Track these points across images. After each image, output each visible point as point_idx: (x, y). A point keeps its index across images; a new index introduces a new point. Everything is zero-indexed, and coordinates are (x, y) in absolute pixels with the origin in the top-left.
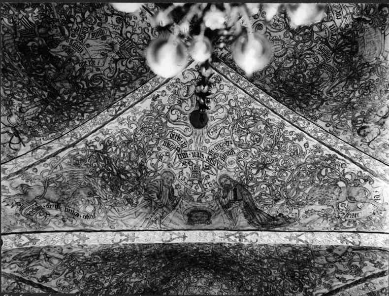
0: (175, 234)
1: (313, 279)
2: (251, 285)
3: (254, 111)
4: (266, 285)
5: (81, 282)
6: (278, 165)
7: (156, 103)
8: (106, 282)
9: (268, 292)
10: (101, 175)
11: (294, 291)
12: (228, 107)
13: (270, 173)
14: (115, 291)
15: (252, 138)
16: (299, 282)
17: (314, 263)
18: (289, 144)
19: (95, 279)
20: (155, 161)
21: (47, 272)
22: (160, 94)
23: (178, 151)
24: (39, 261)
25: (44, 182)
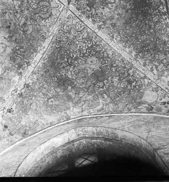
1: (147, 56)
4: (133, 35)
11: (135, 49)
17: (159, 54)
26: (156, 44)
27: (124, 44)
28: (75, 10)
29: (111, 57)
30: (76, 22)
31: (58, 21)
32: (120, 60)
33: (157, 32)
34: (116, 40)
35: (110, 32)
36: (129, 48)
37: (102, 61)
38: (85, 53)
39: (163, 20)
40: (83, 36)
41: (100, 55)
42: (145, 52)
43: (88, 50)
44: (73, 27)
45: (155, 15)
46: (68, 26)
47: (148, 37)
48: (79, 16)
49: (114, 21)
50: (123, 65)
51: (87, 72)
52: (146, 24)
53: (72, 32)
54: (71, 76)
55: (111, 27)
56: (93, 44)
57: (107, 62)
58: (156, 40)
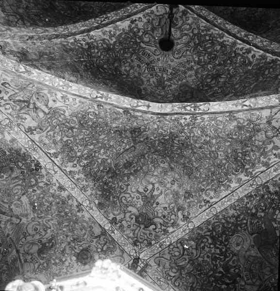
0: (141, 102)
1: (253, 158)
2: (199, 171)
3: (212, 36)
6: (229, 74)
7: (133, 26)
8: (79, 151)
9: (214, 177)
10: (84, 63)
12: (191, 35)
13: (222, 80)
14: (85, 162)
15: (209, 57)
16: (242, 163)
17: (255, 140)
18: (239, 57)
19: (71, 145)
20: (128, 69)
21: (34, 124)
22: (137, 19)
23: (148, 65)
24: (29, 110)
25: (40, 53)
26: (236, 141)
27: (222, 188)
28: (150, 251)
29: (239, 213)
30: (169, 253)
31: (160, 283)
32: (248, 201)
33: (218, 134)
34: (212, 198)
35: (197, 203)
36: (231, 182)
37: (241, 228)
38: (220, 251)
39: (203, 123)
40: (193, 248)
41: (230, 228)
42: (245, 159)
43: (217, 246)
44: (175, 260)
45: (191, 131)
46: (172, 268)
47: (222, 148)
48: (160, 247)
49: (182, 193)
50: (258, 198)
51: (254, 256)
52: (200, 148)
53: (180, 264)
54: (254, 287)
55: (189, 200)
56: (208, 235)
57: (245, 221)
58: (231, 138)
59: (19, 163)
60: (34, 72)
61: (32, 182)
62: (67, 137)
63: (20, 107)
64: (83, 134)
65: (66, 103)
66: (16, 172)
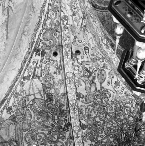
5: (91, 120)
8: (100, 136)
19: (98, 127)
21: (84, 93)
24: (87, 80)
59: (56, 116)
60: (110, 49)
61: (55, 138)
62: (100, 119)
63: (84, 74)
64: (112, 123)
65: (115, 89)
66: (49, 122)
